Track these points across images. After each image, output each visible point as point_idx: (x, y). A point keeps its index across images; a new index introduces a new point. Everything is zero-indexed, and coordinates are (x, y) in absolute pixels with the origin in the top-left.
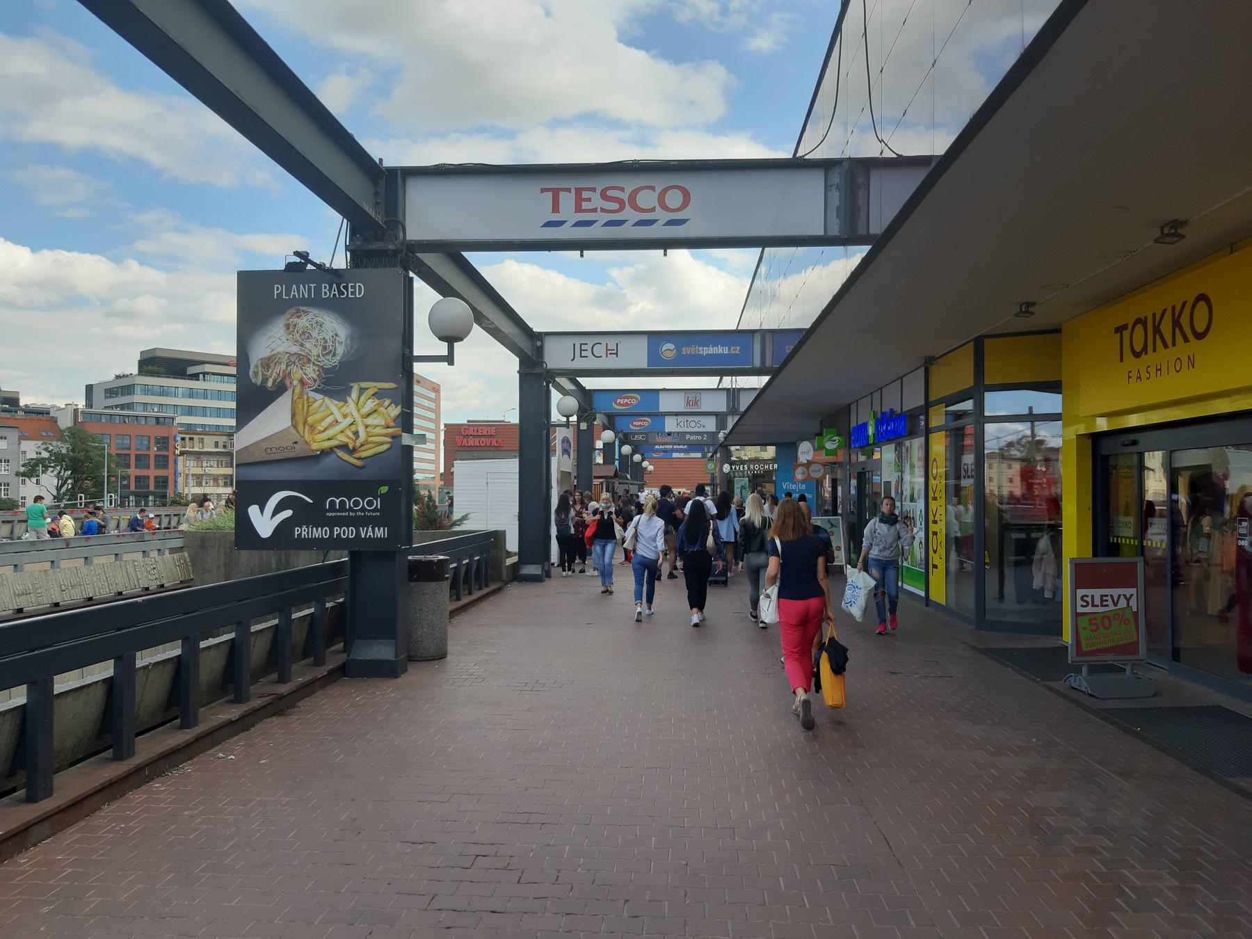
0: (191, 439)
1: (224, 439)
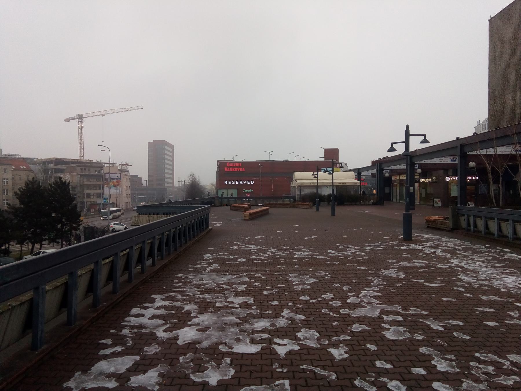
0: (85, 169)
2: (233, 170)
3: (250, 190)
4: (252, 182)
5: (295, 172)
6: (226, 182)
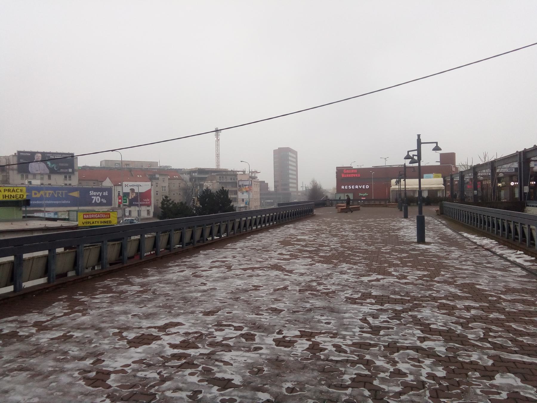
0: (223, 177)
1: (234, 177)
2: (350, 176)
3: (366, 194)
4: (367, 187)
5: (392, 179)
6: (343, 187)
